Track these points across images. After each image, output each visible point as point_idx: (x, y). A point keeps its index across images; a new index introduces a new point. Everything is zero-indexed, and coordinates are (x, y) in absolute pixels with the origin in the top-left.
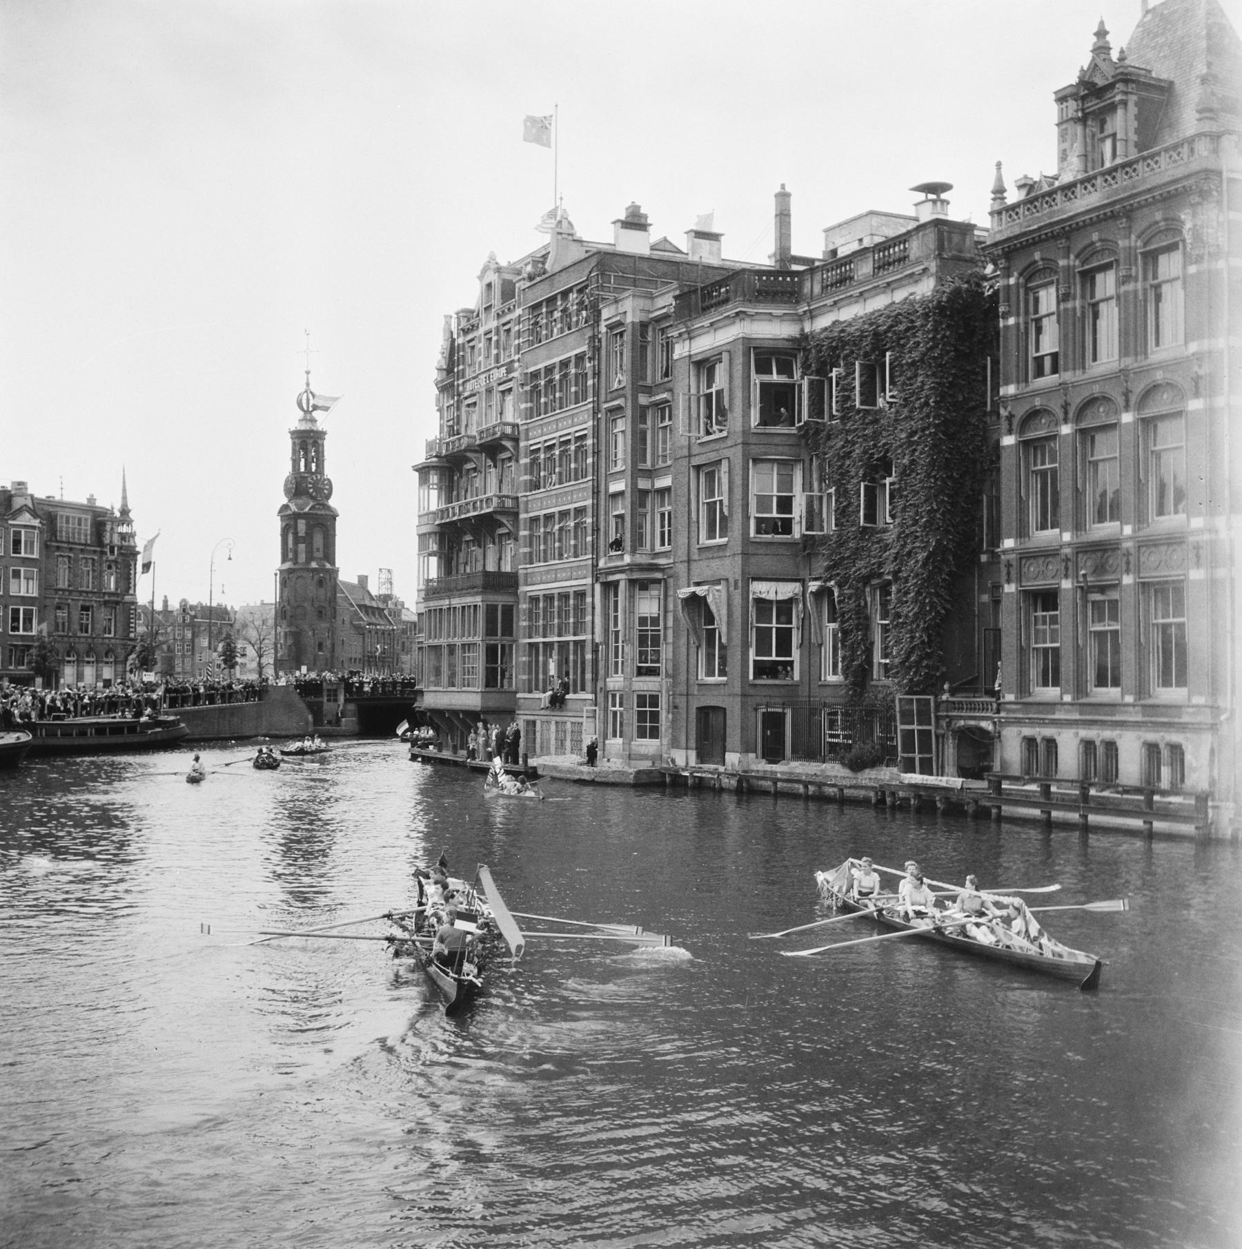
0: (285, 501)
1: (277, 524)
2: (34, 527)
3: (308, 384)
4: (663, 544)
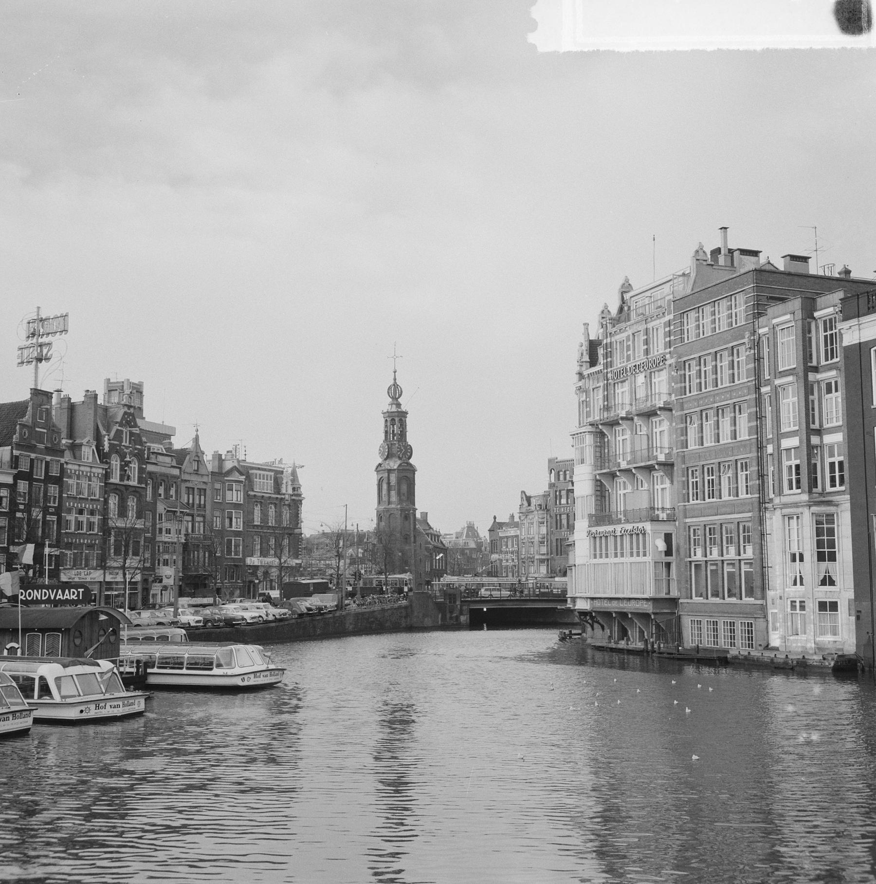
0: (380, 461)
1: (374, 478)
2: (241, 482)
3: (395, 379)
4: (833, 484)
